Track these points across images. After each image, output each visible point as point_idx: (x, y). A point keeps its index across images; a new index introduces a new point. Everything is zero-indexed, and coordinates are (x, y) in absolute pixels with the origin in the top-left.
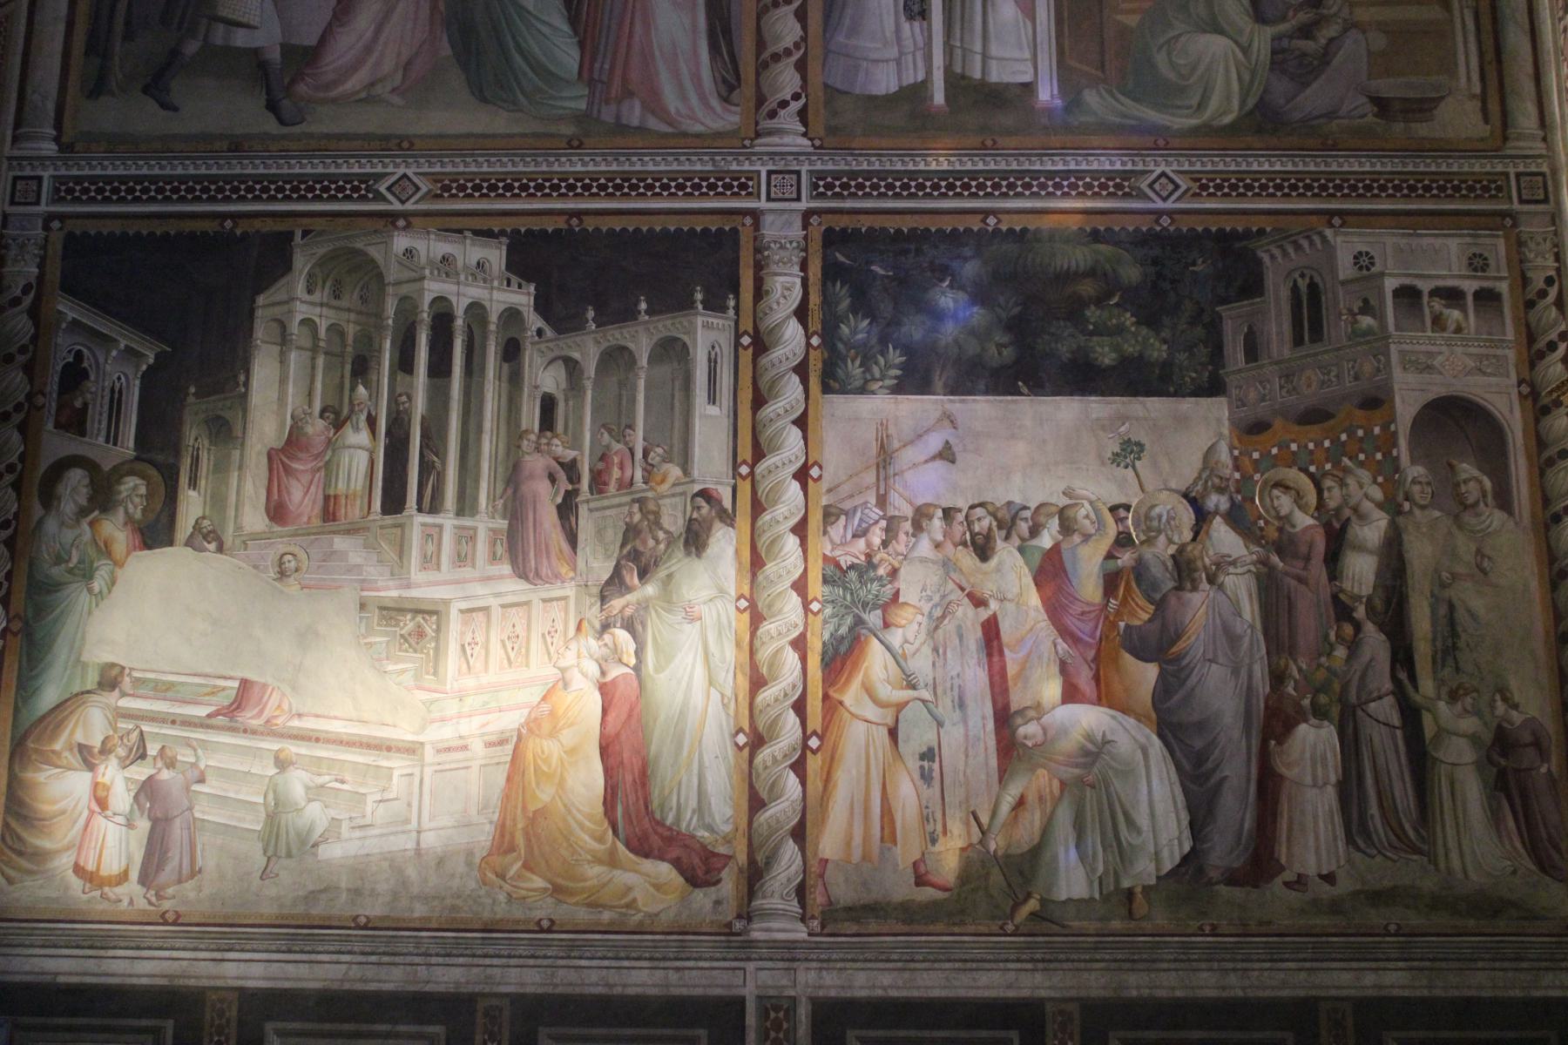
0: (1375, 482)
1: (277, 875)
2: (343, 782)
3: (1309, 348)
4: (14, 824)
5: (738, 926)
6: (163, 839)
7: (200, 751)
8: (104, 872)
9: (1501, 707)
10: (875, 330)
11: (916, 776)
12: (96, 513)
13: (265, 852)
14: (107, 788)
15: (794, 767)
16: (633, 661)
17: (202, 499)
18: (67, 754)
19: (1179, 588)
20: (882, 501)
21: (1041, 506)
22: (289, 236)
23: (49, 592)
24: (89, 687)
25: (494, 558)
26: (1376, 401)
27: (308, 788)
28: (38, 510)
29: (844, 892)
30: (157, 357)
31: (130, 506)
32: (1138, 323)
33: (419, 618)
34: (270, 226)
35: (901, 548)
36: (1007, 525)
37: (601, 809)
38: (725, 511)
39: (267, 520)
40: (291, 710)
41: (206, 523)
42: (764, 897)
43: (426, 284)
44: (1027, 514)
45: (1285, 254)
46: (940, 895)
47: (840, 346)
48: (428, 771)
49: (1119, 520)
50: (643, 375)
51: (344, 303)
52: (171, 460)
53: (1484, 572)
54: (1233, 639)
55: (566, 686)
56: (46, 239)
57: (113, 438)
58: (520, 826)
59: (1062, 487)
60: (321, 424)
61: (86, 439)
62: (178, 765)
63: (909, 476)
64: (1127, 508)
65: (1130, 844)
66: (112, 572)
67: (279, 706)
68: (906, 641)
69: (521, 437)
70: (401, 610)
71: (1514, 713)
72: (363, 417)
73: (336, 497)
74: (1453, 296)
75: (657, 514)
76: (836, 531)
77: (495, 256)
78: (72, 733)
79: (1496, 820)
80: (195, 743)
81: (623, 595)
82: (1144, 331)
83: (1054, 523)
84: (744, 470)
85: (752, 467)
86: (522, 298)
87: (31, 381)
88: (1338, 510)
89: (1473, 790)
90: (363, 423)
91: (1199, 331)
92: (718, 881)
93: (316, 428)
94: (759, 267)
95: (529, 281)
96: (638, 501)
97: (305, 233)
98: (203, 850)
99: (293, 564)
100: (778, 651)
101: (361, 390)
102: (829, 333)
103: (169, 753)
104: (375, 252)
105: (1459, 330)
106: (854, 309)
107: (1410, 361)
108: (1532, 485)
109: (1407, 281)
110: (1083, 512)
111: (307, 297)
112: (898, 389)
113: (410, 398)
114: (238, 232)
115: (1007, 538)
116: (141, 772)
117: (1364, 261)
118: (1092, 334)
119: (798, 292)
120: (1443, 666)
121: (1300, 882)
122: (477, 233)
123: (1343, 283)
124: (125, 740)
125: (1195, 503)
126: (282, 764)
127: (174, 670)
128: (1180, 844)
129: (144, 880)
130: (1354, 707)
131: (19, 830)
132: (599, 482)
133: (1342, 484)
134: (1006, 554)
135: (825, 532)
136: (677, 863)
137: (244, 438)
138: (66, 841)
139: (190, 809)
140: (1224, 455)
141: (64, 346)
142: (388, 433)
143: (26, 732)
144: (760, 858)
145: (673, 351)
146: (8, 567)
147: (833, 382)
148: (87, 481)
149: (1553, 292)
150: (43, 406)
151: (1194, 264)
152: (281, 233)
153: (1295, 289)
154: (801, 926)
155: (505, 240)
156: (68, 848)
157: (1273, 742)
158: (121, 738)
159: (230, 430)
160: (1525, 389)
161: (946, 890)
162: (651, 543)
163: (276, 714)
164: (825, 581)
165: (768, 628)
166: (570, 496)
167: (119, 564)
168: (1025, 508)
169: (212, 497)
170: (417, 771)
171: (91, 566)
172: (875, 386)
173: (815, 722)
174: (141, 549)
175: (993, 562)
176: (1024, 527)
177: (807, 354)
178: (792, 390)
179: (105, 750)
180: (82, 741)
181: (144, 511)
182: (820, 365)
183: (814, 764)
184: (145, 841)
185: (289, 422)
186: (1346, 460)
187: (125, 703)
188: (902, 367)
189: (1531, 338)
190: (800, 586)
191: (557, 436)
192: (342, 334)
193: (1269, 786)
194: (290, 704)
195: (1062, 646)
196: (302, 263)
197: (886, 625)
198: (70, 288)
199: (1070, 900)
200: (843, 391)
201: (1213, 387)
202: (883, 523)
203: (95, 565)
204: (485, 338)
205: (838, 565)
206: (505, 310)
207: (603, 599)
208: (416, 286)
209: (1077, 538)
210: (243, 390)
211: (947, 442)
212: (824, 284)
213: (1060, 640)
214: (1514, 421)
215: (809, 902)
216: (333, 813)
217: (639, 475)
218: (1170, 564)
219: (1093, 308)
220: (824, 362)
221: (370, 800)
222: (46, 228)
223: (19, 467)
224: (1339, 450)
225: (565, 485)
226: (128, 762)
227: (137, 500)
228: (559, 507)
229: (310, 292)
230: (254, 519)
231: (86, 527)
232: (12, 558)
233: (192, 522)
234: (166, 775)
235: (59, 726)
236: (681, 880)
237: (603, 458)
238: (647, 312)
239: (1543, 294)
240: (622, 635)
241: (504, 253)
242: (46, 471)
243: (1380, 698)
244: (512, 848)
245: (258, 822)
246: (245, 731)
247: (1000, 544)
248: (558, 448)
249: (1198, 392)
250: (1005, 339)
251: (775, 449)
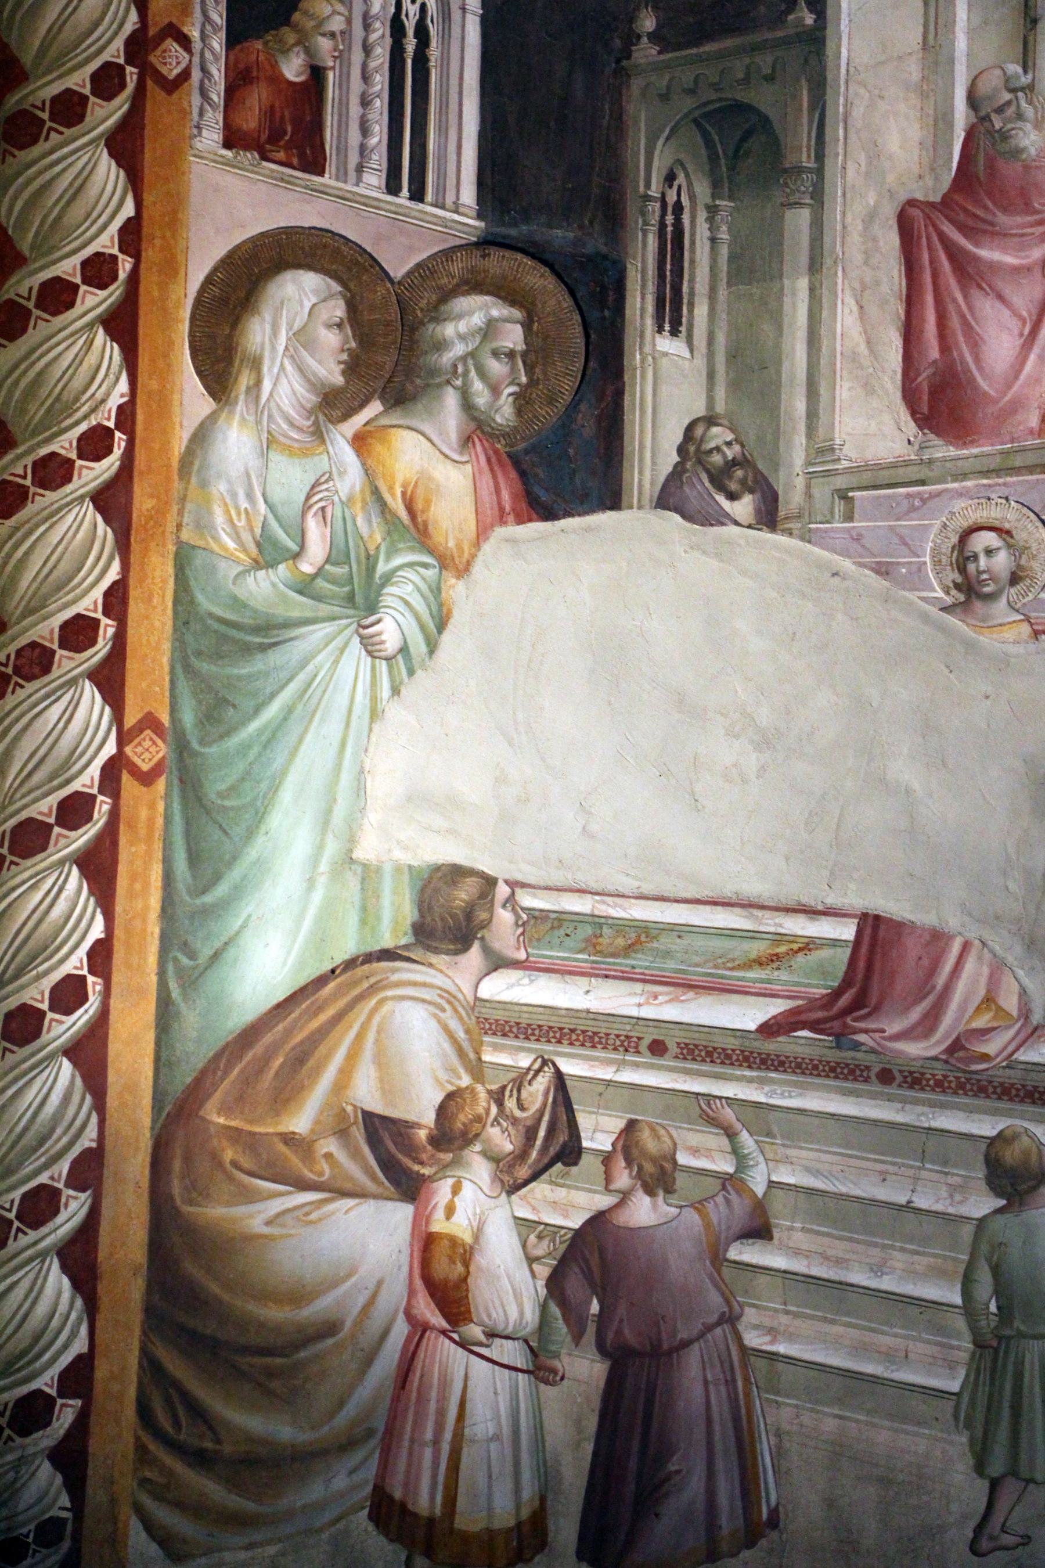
1: (1026, 1540)
6: (648, 1416)
7: (746, 1139)
12: (375, 407)
13: (980, 1467)
17: (700, 362)
18: (330, 1145)
23: (247, 650)
24: (387, 941)
31: (478, 385)
39: (911, 427)
40: (1025, 1013)
41: (719, 435)
52: (596, 244)
61: (326, 180)
62: (681, 1181)
66: (437, 590)
67: (989, 1000)
78: (342, 1083)
80: (729, 1114)
98: (779, 1453)
99: (1002, 561)
103: (645, 1137)
124: (510, 1104)
127: (647, 888)
137: (820, 171)
138: (342, 1419)
139: (730, 1319)
143: (198, 1081)
146: (114, 573)
148: (338, 310)
150: (186, 74)
156: (347, 1444)
158: (498, 1097)
159: (775, 148)
163: (980, 1023)
169: (733, 356)
171: (370, 569)
174: (520, 520)
180: (378, 1107)
181: (522, 401)
184: (592, 1423)
185: (961, 115)
194: (1023, 992)
203: (382, 568)
210: (809, 19)
223: (125, 265)
226: (523, 1172)
227: (497, 368)
231: (348, 455)
232: (123, 546)
233: (672, 435)
242: (209, 281)
245: (951, 1366)
246: (886, 1077)
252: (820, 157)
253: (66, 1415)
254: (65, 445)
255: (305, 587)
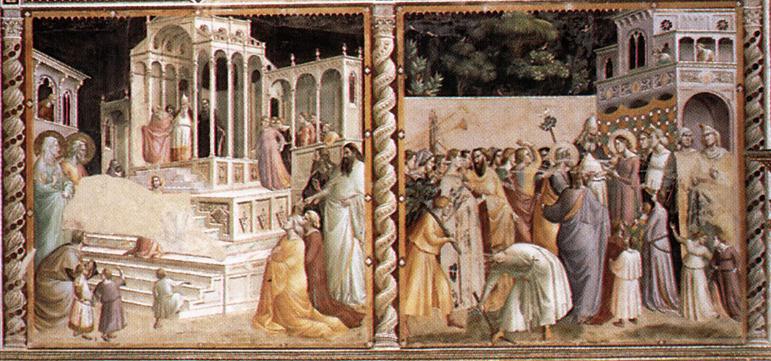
0: (665, 135)
2: (188, 283)
3: (637, 70)
4: (38, 304)
5: (370, 345)
8: (83, 325)
9: (717, 242)
10: (429, 64)
11: (448, 275)
14: (81, 288)
15: (392, 274)
16: (318, 226)
18: (60, 273)
19: (571, 187)
20: (432, 148)
21: (506, 150)
22: (145, 19)
25: (253, 178)
26: (667, 96)
27: (173, 287)
28: (35, 158)
29: (415, 328)
30: (85, 81)
32: (555, 59)
33: (219, 207)
34: (133, 14)
35: (443, 172)
36: (491, 159)
37: (305, 294)
38: (358, 153)
42: (381, 332)
43: (212, 43)
44: (499, 153)
45: (628, 22)
46: (457, 329)
47: (413, 73)
48: (227, 278)
49: (543, 156)
50: (319, 88)
51: (174, 53)
53: (712, 176)
54: (594, 211)
55: (288, 238)
56: (24, 21)
57: (67, 121)
58: (270, 301)
59: (515, 140)
60: (165, 114)
63: (445, 136)
64: (547, 149)
65: (546, 308)
67: (157, 250)
68: (444, 215)
69: (262, 120)
70: (211, 203)
71: (723, 245)
72: (186, 110)
73: (176, 149)
74: (708, 42)
75: (328, 155)
76: (411, 163)
77: (245, 28)
79: (710, 289)
81: (312, 195)
82: (558, 62)
83: (513, 158)
84: (368, 134)
85: (372, 133)
86: (259, 50)
87: (24, 94)
88: (647, 149)
89: (701, 281)
90: (186, 114)
91: (585, 62)
92: (360, 325)
93: (164, 116)
94: (373, 33)
95: (263, 41)
96: (320, 149)
97: (152, 18)
100: (386, 220)
101: (184, 97)
102: (407, 66)
104: (186, 27)
105: (710, 60)
106: (419, 54)
107: (686, 76)
108: (739, 136)
109: (687, 35)
110: (526, 152)
111: (155, 51)
112: (439, 94)
113: (208, 101)
114: (118, 17)
115: (491, 165)
116: (95, 281)
117: (667, 25)
118: (533, 64)
119: (391, 47)
120: (692, 222)
121: (620, 323)
122: (235, 17)
123: (655, 36)
125: (579, 146)
126: (160, 276)
128: (567, 305)
129: (102, 328)
130: (649, 243)
131: (44, 309)
132: (299, 142)
133: (649, 136)
134: (490, 172)
135: (406, 163)
136: (340, 317)
139: (120, 297)
140: (593, 123)
141: (37, 77)
142: (199, 117)
144: (379, 315)
145: (333, 75)
147: (409, 91)
149: (758, 39)
151: (584, 28)
152: (140, 18)
153: (632, 40)
154: (396, 344)
155: (249, 21)
157: (611, 260)
160: (740, 88)
161: (461, 327)
162: (325, 170)
164: (407, 186)
165: (381, 209)
166: (287, 147)
167: (75, 183)
168: (499, 150)
170: (222, 278)
172: (429, 93)
173: (402, 253)
175: (484, 176)
176: (498, 159)
177: (397, 77)
178: (390, 93)
179: (78, 271)
182: (402, 82)
183: (402, 272)
185: (151, 113)
186: (652, 126)
187: (85, 249)
188: (442, 82)
189: (745, 62)
190: (395, 189)
191: (279, 119)
192: (173, 69)
193: (609, 281)
195: (516, 216)
196: (151, 33)
197: (435, 207)
198: (36, 46)
199: (517, 331)
200: (415, 96)
201: (590, 90)
202: (433, 159)
204: (243, 72)
205: (412, 179)
206: (252, 56)
207: (305, 196)
208: (208, 44)
209: (522, 165)
211: (463, 120)
212: (405, 41)
213: (514, 214)
214: (734, 106)
215: (401, 334)
216: (185, 298)
217: (318, 139)
218: (566, 176)
219: (534, 52)
220: (405, 81)
221: (201, 291)
222: (23, 16)
224: (649, 120)
225: (284, 142)
228: (282, 153)
229: (156, 48)
230: (138, 161)
231: (58, 166)
232: (25, 181)
233: (109, 162)
234: (107, 282)
235: (55, 261)
236: (343, 326)
237: (301, 129)
238: (320, 56)
239: (753, 40)
240: (314, 214)
241: (249, 27)
243: (662, 238)
244: (267, 312)
247: (488, 168)
248: (281, 126)
249: (583, 93)
250: (491, 68)
251: (382, 122)
252: (130, 118)
253: (24, 312)
254: (16, 165)
255: (53, 187)
